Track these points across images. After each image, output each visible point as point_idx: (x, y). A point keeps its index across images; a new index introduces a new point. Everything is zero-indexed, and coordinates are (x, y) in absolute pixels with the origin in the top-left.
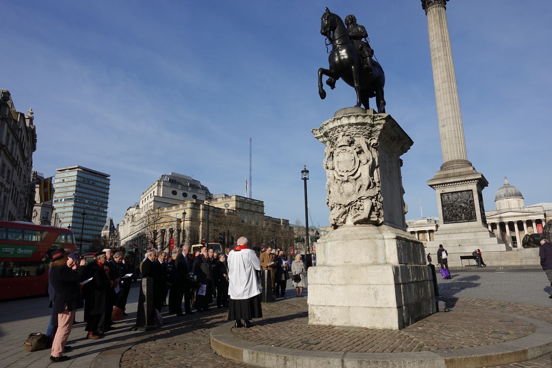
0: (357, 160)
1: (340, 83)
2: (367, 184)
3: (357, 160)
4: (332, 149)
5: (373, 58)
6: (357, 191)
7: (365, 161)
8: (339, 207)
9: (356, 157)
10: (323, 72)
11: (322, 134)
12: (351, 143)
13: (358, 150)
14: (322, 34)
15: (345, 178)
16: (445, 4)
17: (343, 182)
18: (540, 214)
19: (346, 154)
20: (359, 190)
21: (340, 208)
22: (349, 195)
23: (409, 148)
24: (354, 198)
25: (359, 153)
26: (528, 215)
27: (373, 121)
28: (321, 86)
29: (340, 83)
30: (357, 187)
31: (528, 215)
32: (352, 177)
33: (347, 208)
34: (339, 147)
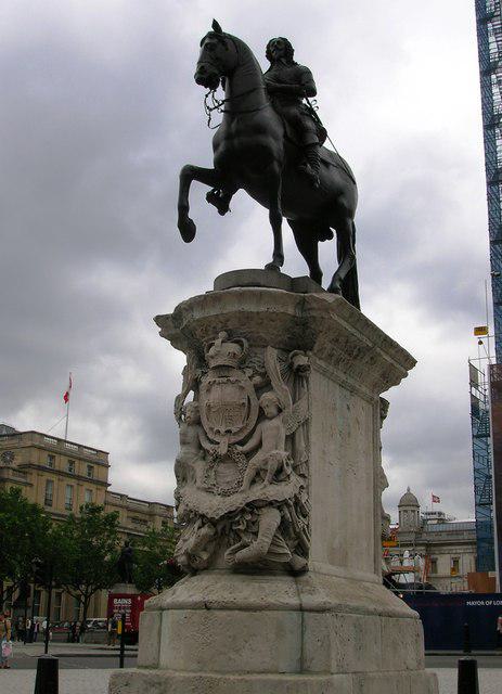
1: (242, 199)
2: (272, 466)
4: (199, 371)
5: (327, 144)
6: (246, 483)
7: (272, 410)
8: (198, 523)
9: (253, 397)
10: (190, 175)
11: (178, 331)
12: (242, 364)
13: (257, 379)
14: (200, 81)
15: (223, 450)
17: (218, 459)
19: (229, 389)
20: (253, 482)
21: (203, 524)
22: (225, 494)
23: (406, 375)
24: (237, 501)
25: (259, 389)
27: (303, 310)
28: (183, 208)
29: (242, 199)
30: (249, 473)
32: (240, 448)
33: (219, 528)
34: (215, 368)
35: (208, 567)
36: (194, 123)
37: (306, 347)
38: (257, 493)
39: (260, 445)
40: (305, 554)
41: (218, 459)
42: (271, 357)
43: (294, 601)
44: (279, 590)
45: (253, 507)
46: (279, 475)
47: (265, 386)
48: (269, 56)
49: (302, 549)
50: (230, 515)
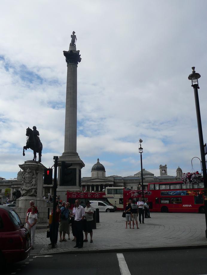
0: (32, 177)
3: (32, 177)
12: (31, 172)
13: (33, 174)
15: (28, 182)
16: (78, 64)
18: (112, 182)
20: (32, 186)
22: (28, 187)
24: (30, 188)
25: (33, 175)
26: (106, 182)
28: (24, 152)
31: (106, 182)
35: (26, 195)
36: (24, 140)
37: (38, 170)
38: (32, 187)
39: (32, 182)
40: (37, 194)
41: (27, 183)
42: (34, 172)
43: (36, 199)
44: (34, 198)
45: (32, 189)
46: (35, 185)
47: (33, 175)
48: (33, 129)
49: (36, 194)
50: (29, 190)
